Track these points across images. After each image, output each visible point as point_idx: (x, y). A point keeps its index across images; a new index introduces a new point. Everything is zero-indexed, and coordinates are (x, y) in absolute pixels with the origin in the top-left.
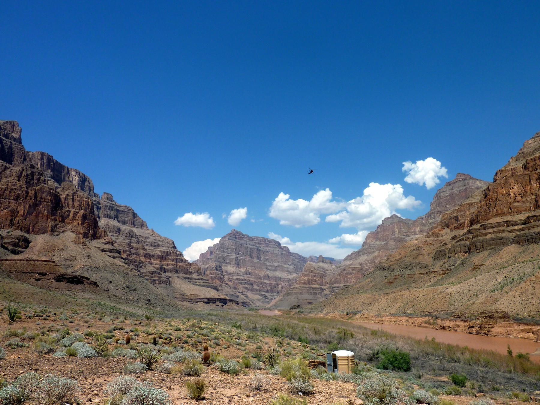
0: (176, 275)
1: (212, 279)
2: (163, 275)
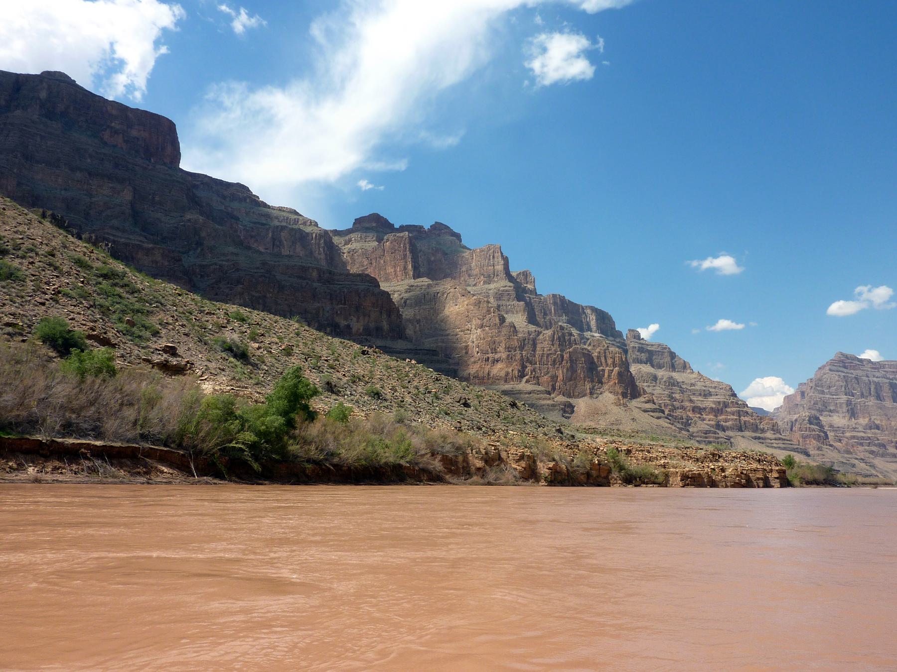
0: (740, 433)
1: (804, 437)
2: (721, 434)
